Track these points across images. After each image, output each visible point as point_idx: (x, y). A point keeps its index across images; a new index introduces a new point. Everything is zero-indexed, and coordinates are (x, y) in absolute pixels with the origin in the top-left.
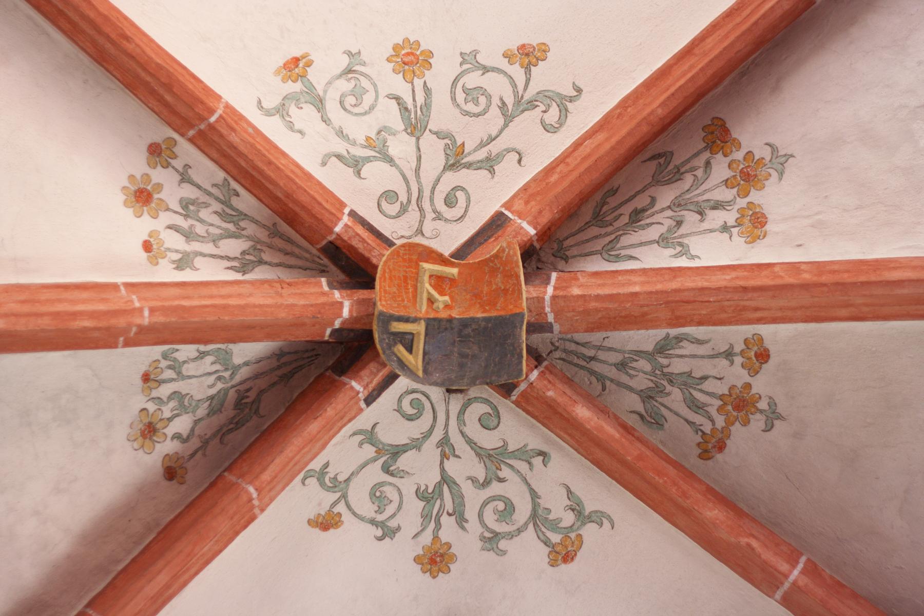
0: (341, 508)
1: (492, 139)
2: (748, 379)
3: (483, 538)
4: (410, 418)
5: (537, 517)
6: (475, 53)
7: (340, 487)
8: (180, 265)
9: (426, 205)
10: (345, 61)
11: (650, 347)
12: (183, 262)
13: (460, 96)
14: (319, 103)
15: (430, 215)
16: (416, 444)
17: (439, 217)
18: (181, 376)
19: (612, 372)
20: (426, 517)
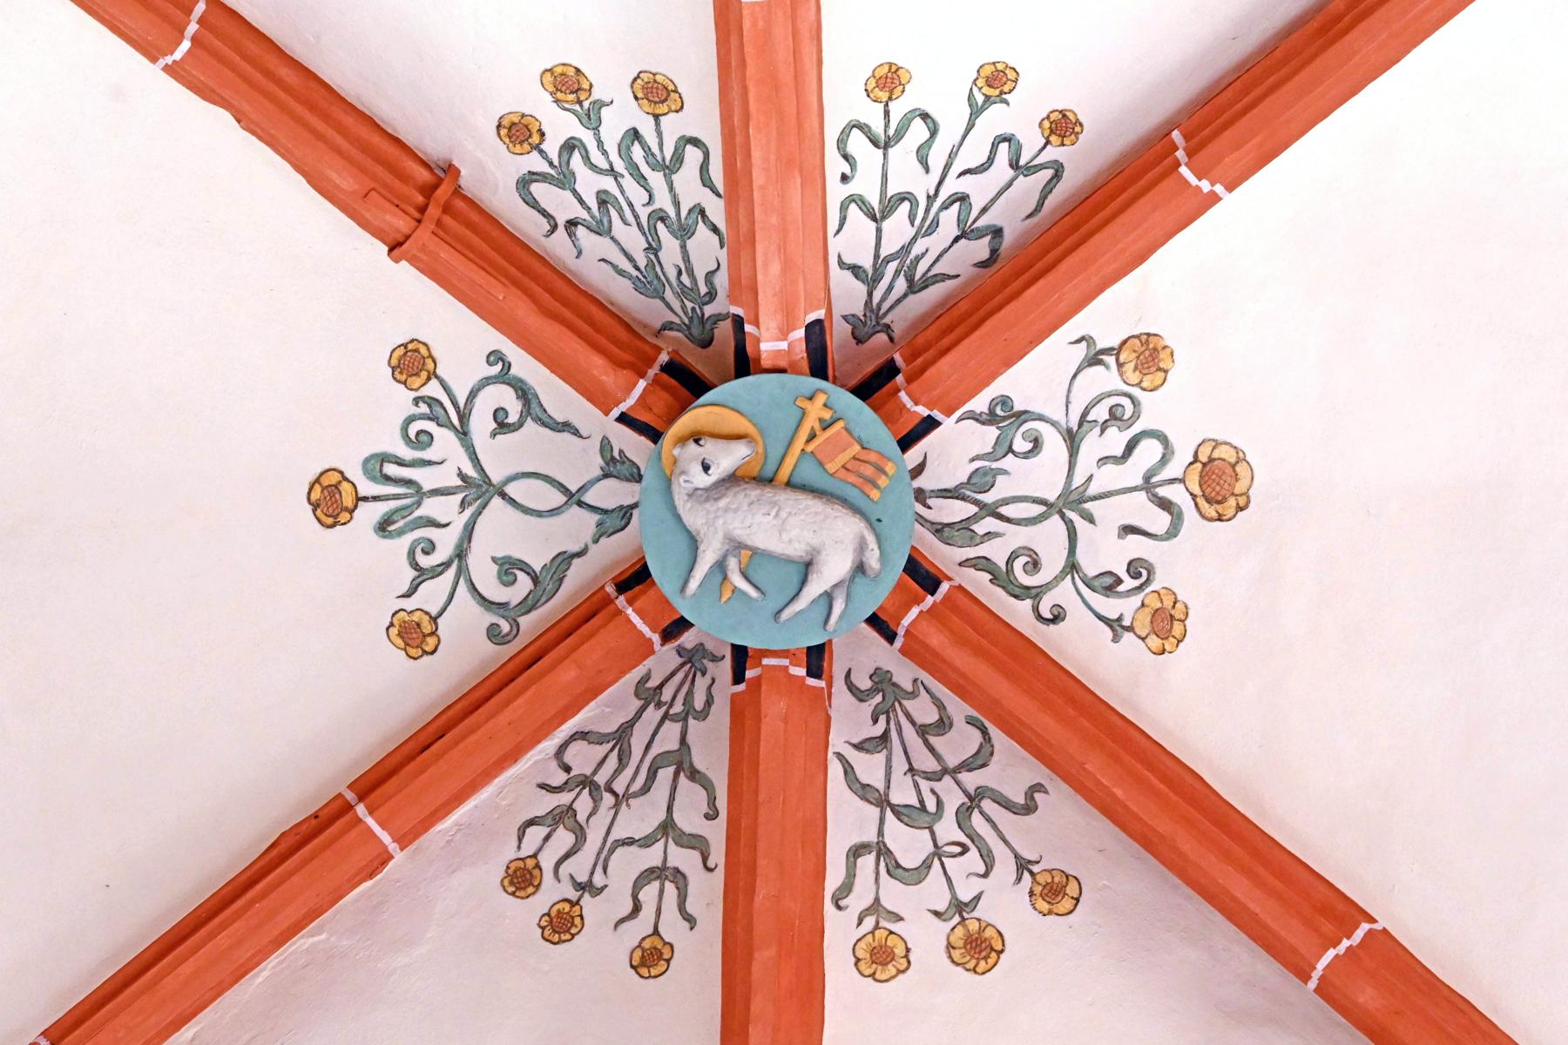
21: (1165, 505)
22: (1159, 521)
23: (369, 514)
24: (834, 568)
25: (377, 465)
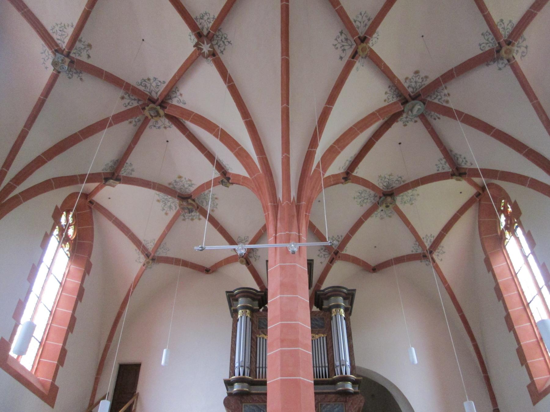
21: (417, 76)
22: (418, 77)
23: (407, 123)
24: (419, 107)
25: (403, 123)
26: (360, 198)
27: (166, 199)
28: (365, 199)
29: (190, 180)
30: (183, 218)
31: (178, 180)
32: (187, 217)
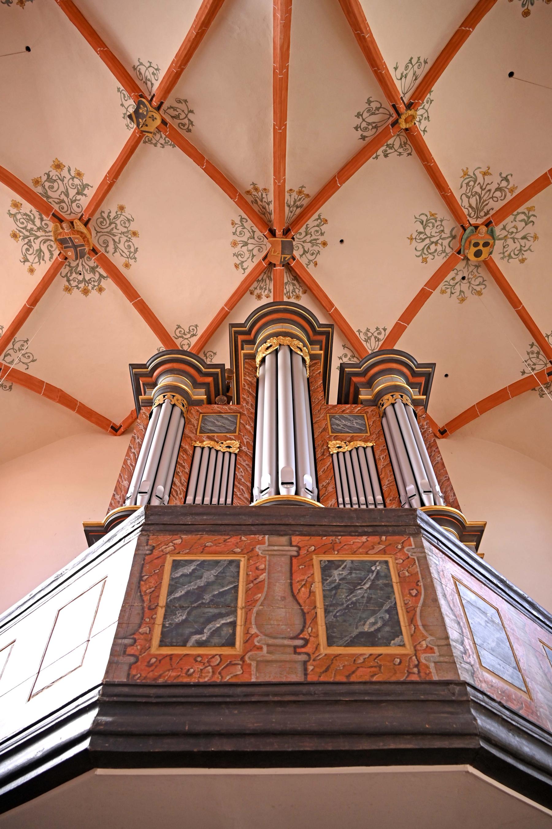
0: (313, 261)
1: (249, 231)
2: (295, 192)
3: (321, 236)
4: (299, 248)
5: (318, 226)
6: (233, 232)
7: (310, 261)
8: (271, 292)
9: (261, 243)
10: (235, 257)
11: (288, 208)
12: (270, 290)
13: (241, 236)
14: (243, 262)
15: (262, 243)
16: (303, 247)
17: (263, 241)
18: (289, 292)
19: (292, 214)
20: (317, 245)
26: (423, 240)
27: (32, 229)
28: (433, 243)
29: (79, 174)
30: (67, 284)
31: (54, 173)
32: (76, 284)
